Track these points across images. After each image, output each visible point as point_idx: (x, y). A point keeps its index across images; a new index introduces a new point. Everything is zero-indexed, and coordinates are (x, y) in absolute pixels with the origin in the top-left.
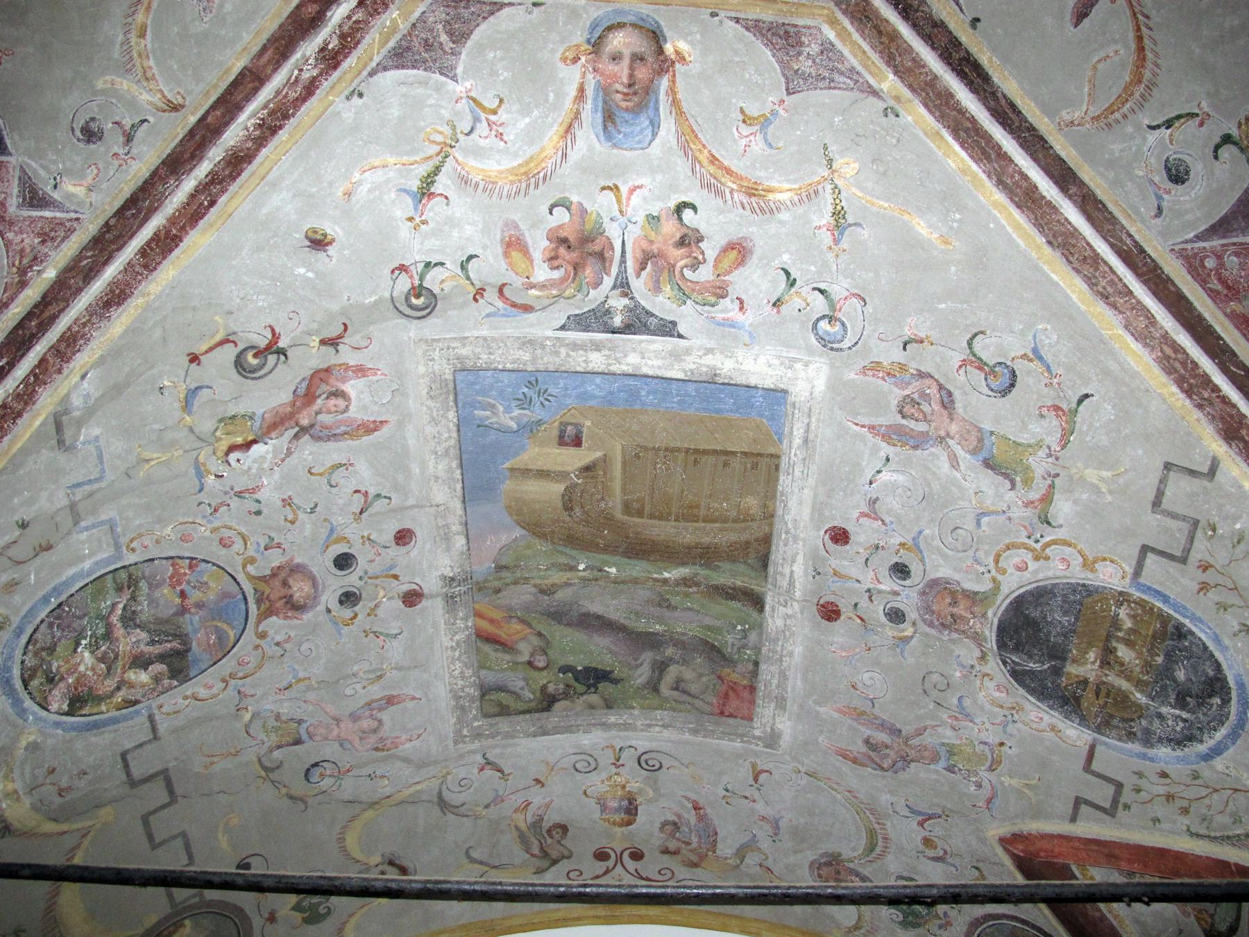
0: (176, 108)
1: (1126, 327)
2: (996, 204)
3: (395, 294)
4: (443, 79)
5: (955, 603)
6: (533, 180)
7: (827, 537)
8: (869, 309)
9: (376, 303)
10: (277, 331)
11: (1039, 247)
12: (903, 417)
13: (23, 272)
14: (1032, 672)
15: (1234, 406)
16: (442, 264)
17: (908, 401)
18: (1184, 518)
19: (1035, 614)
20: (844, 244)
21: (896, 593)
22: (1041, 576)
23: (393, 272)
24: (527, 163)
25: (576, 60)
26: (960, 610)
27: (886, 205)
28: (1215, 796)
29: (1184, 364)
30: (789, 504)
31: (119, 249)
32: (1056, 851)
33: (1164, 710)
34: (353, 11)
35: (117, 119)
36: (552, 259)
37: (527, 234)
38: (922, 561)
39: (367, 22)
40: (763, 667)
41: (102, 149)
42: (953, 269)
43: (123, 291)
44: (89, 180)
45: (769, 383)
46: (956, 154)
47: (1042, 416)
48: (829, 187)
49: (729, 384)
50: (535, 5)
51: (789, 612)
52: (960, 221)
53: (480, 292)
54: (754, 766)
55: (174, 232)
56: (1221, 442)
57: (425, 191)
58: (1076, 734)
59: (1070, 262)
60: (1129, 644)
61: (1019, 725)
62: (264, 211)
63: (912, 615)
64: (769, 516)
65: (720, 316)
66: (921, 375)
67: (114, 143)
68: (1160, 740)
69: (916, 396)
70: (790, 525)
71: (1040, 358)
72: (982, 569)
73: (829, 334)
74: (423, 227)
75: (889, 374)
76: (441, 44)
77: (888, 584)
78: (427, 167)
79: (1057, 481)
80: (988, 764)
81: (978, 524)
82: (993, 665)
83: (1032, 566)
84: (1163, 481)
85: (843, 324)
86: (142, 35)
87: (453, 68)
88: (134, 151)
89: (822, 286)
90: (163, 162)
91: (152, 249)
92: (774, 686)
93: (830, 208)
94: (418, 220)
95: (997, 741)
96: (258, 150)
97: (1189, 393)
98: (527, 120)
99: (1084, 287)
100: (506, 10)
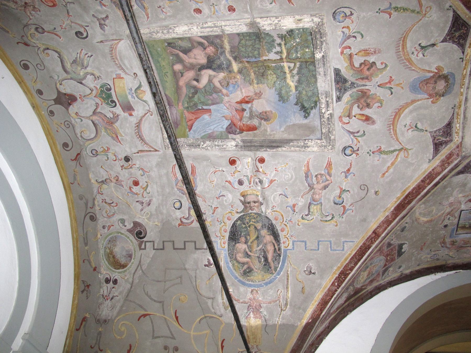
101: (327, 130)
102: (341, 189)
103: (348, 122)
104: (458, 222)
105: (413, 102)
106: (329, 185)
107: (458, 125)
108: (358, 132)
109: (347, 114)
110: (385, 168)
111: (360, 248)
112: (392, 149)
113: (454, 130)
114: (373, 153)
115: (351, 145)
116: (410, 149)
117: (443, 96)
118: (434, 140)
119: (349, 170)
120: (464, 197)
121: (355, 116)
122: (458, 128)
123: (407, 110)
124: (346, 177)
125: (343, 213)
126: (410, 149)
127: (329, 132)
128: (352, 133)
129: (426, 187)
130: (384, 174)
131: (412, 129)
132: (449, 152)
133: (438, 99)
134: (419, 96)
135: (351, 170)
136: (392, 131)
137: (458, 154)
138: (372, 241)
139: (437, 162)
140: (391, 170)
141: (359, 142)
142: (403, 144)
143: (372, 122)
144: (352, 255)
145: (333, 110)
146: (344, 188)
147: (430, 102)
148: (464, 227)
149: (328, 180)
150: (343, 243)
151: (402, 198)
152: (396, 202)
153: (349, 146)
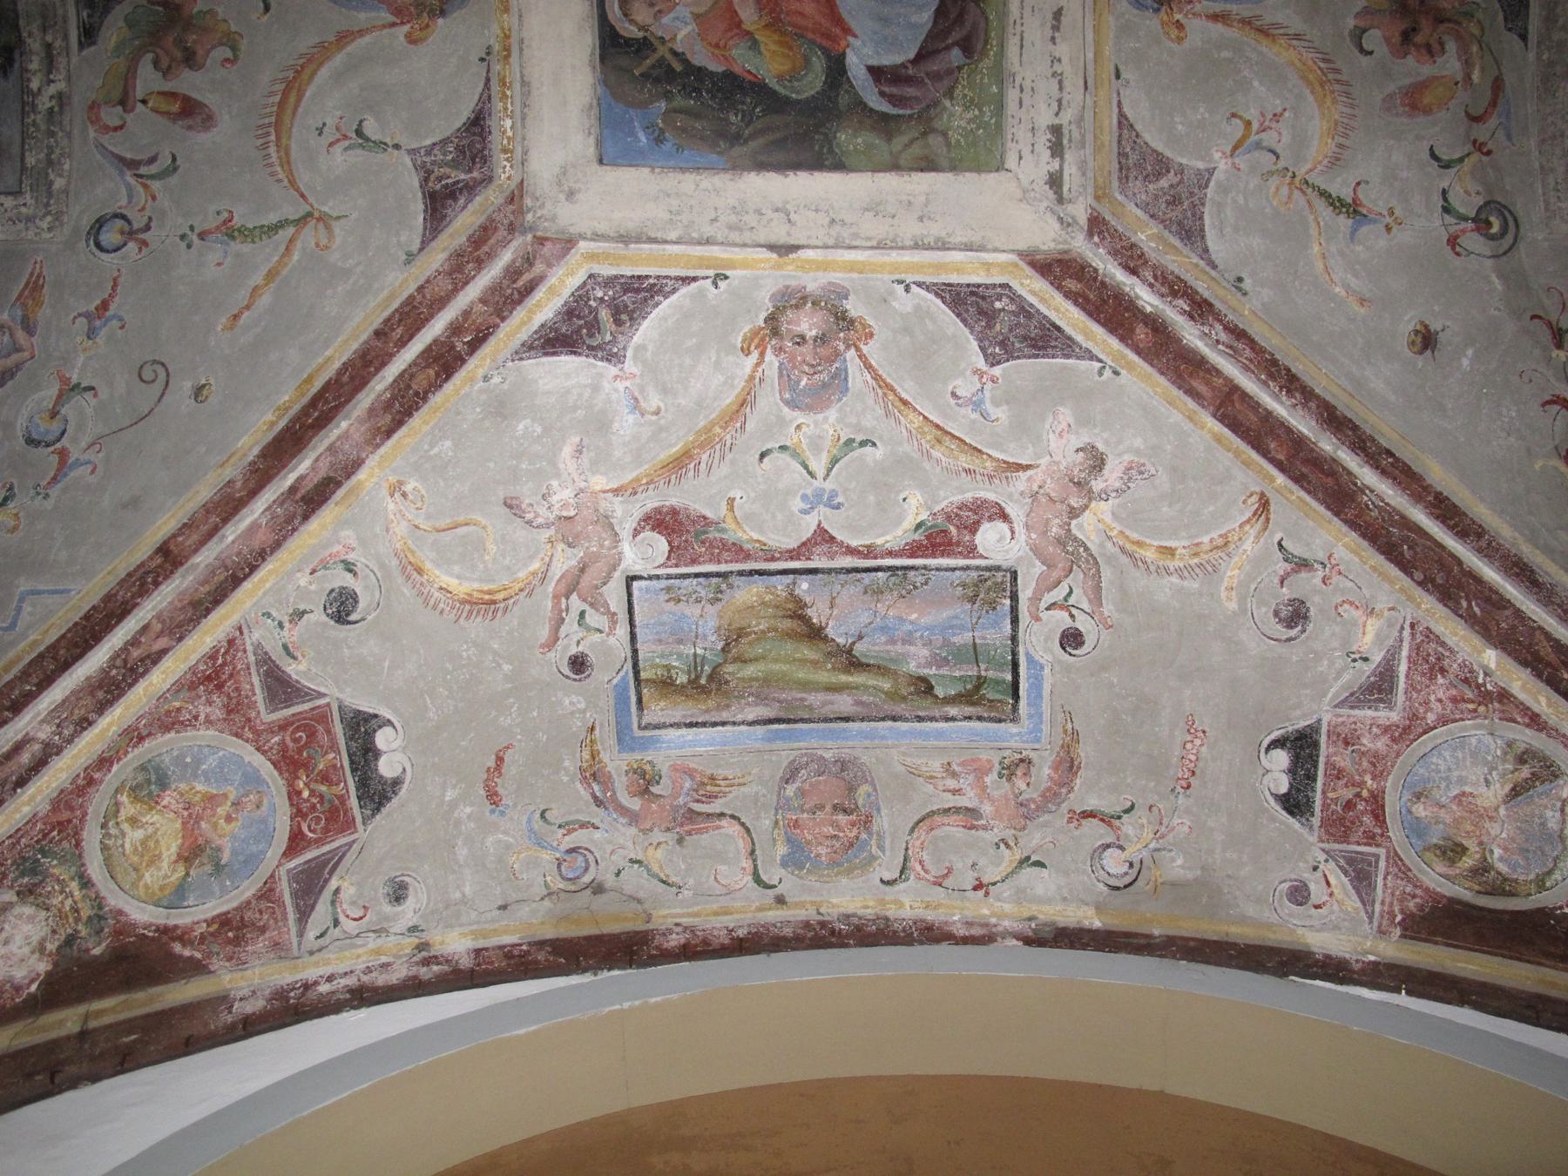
0: (1264, 504)
3: (1489, 253)
4: (1212, 184)
6: (1331, 76)
9: (1501, 276)
10: (1548, 398)
13: (1485, 697)
16: (1444, 192)
23: (1458, 254)
24: (1309, 83)
25: (1180, 26)
31: (1460, 563)
34: (1144, 281)
35: (1276, 581)
36: (1431, 51)
37: (1400, 83)
39: (1155, 268)
41: (1317, 599)
43: (1516, 564)
44: (1356, 614)
50: (1118, 76)
53: (1478, 146)
55: (1430, 498)
57: (1352, 209)
62: (1393, 398)
67: (1307, 585)
74: (1397, 213)
76: (1172, 186)
78: (1320, 204)
86: (1171, 552)
87: (1199, 173)
88: (1321, 556)
90: (1337, 514)
91: (1456, 525)
94: (1388, 220)
96: (1318, 397)
98: (1256, 84)
100: (1126, 110)
101: (42, 156)
102: (64, 380)
103: (118, 123)
104: (635, 652)
105: (344, 38)
106: (18, 366)
107: (508, 123)
108: (152, 160)
109: (116, 94)
110: (243, 295)
111: (87, 617)
112: (273, 218)
113: (496, 141)
114: (202, 236)
115: (124, 211)
116: (338, 218)
117: (443, 13)
118: (426, 180)
119: (105, 306)
120: (616, 491)
121: (144, 102)
122: (510, 133)
123: (324, 72)
124: (91, 334)
125: (54, 480)
126: (338, 218)
127: (50, 163)
128: (133, 165)
129: (392, 355)
130: (236, 317)
131: (347, 143)
132: (481, 219)
133: (427, 26)
134: (362, 16)
135: (113, 307)
136: (272, 149)
137: (511, 224)
138: (142, 585)
139: (437, 258)
140: (265, 300)
141: (154, 198)
142: (311, 200)
143: (204, 121)
144: (42, 648)
145: (69, 79)
146: (74, 380)
147: (402, 38)
148: (666, 685)
149: (18, 349)
150: (22, 600)
151: (297, 408)
152: (273, 424)
153: (116, 216)
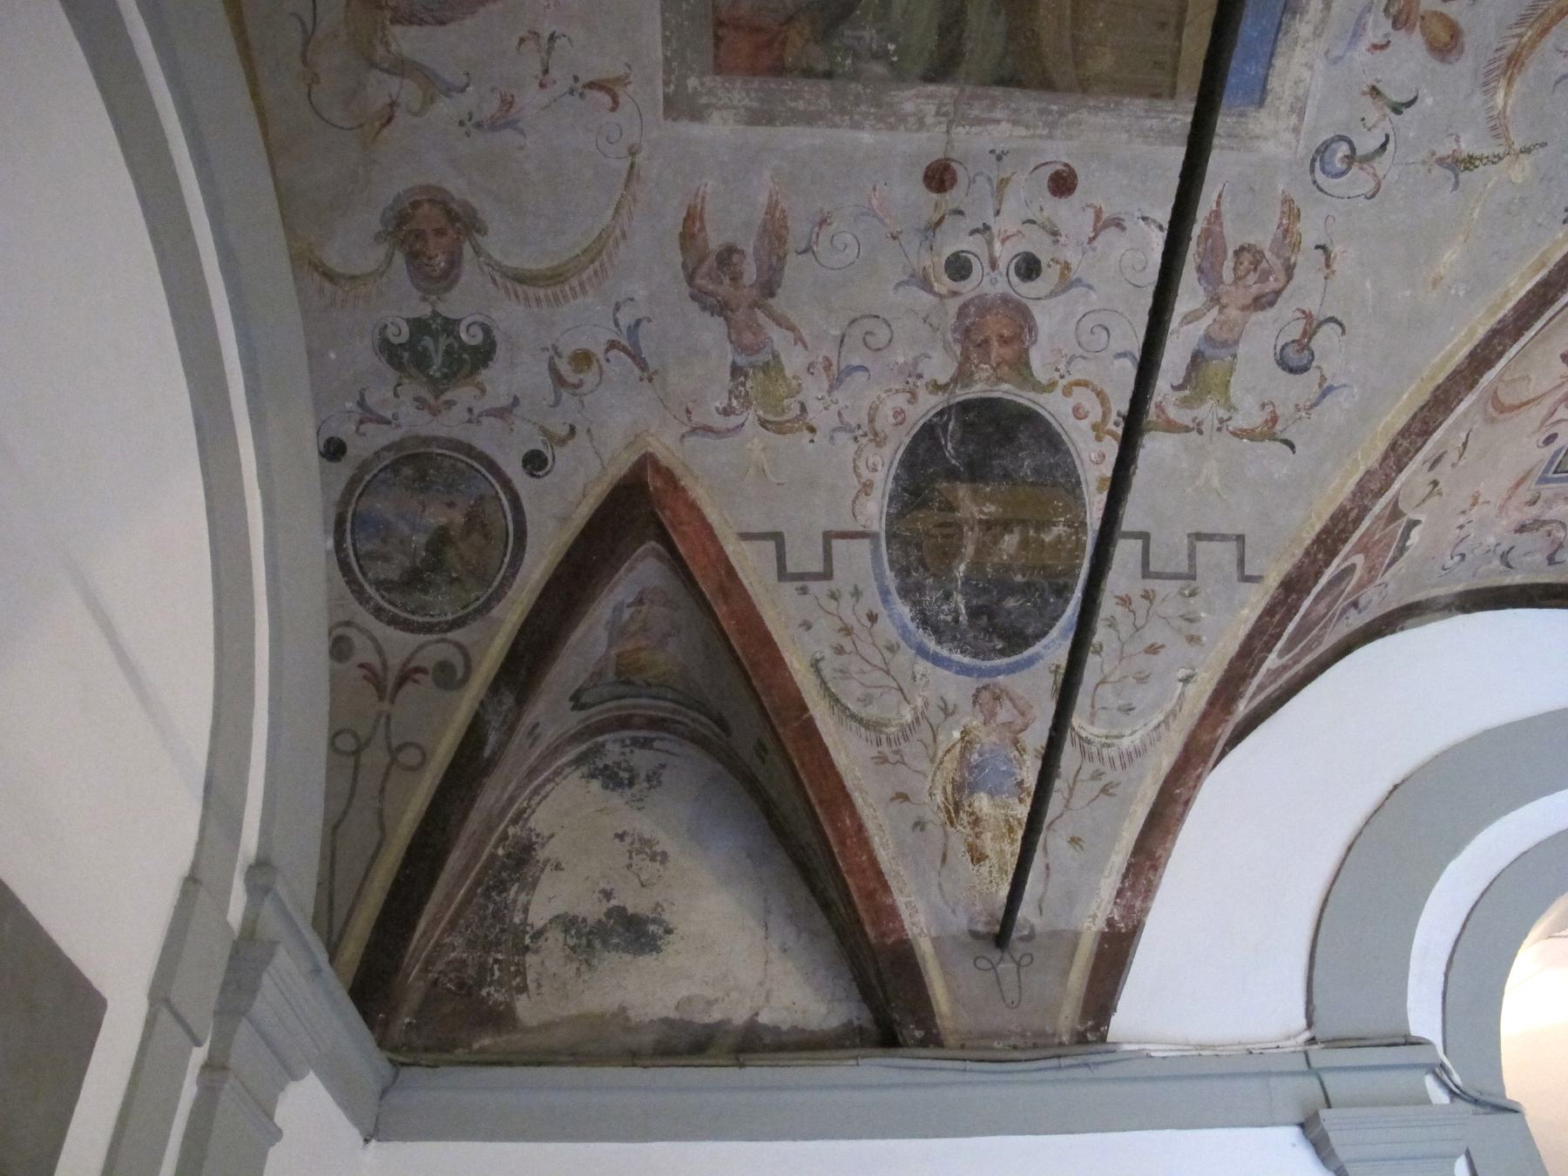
1: (1368, 472)
2: (1472, 331)
5: (1004, 341)
7: (1060, 167)
8: (1362, 202)
11: (1432, 378)
12: (1236, 253)
14: (940, 448)
15: (1316, 582)
17: (1257, 255)
18: (1192, 565)
19: (1023, 437)
20: (1438, 171)
21: (993, 265)
22: (1074, 436)
26: (996, 350)
27: (1475, 215)
28: (878, 674)
29: (1343, 531)
30: (1102, 114)
32: (686, 528)
33: (959, 600)
38: (1053, 294)
40: (825, 86)
42: (1408, 293)
45: (1274, 83)
46: (1523, 285)
47: (1263, 406)
48: (1501, 151)
49: (1278, 31)
51: (929, 120)
52: (1457, 295)
54: (623, 81)
56: (1279, 579)
58: (874, 512)
59: (1422, 408)
60: (1024, 544)
61: (853, 447)
63: (968, 288)
64: (1084, 86)
65: (1370, 19)
66: (1289, 270)
68: (914, 604)
69: (1264, 265)
70: (1071, 116)
71: (1324, 395)
72: (1062, 367)
73: (1334, 153)
75: (1286, 231)
77: (1005, 253)
79: (1194, 434)
80: (770, 417)
81: (1119, 355)
82: (928, 405)
83: (1085, 425)
84: (1224, 538)
85: (1343, 173)
89: (1390, 147)
92: (793, 105)
93: (1477, 153)
95: (814, 423)
97: (1318, 540)
99: (1399, 426)
